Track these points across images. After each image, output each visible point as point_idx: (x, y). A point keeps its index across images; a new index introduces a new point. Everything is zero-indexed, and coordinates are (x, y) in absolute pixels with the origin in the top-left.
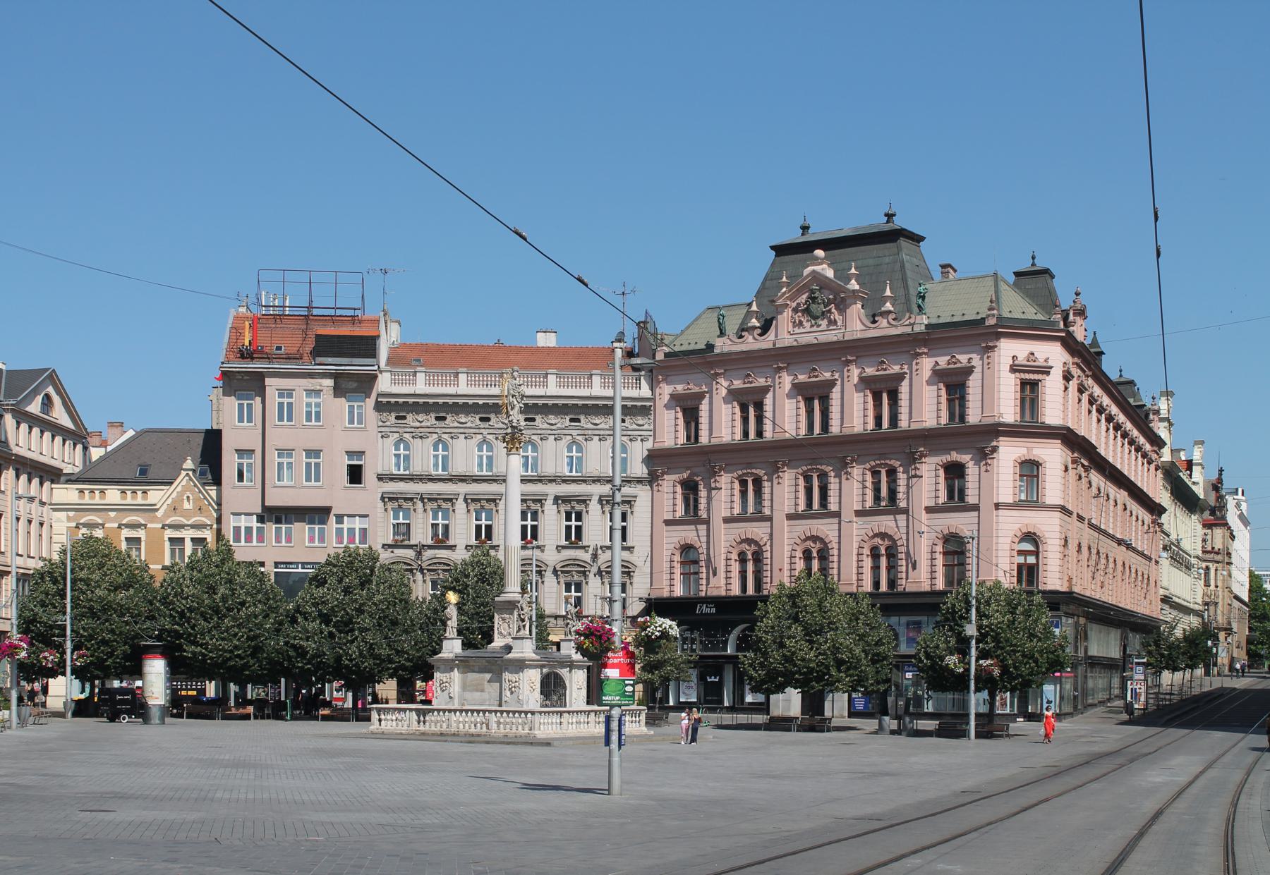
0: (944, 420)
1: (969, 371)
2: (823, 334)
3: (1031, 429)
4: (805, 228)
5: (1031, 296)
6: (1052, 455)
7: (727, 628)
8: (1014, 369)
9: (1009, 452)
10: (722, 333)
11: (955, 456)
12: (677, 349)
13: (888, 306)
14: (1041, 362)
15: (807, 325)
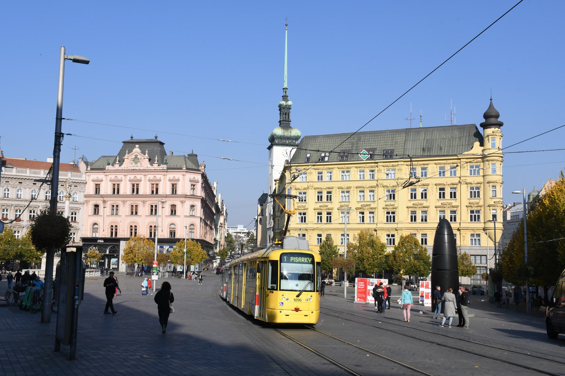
0: (171, 193)
1: (178, 180)
2: (138, 167)
3: (193, 196)
4: (132, 138)
5: (192, 161)
6: (198, 204)
7: (106, 246)
8: (190, 181)
9: (189, 202)
10: (109, 164)
11: (175, 203)
12: (93, 167)
13: (156, 162)
14: (196, 179)
15: (134, 164)
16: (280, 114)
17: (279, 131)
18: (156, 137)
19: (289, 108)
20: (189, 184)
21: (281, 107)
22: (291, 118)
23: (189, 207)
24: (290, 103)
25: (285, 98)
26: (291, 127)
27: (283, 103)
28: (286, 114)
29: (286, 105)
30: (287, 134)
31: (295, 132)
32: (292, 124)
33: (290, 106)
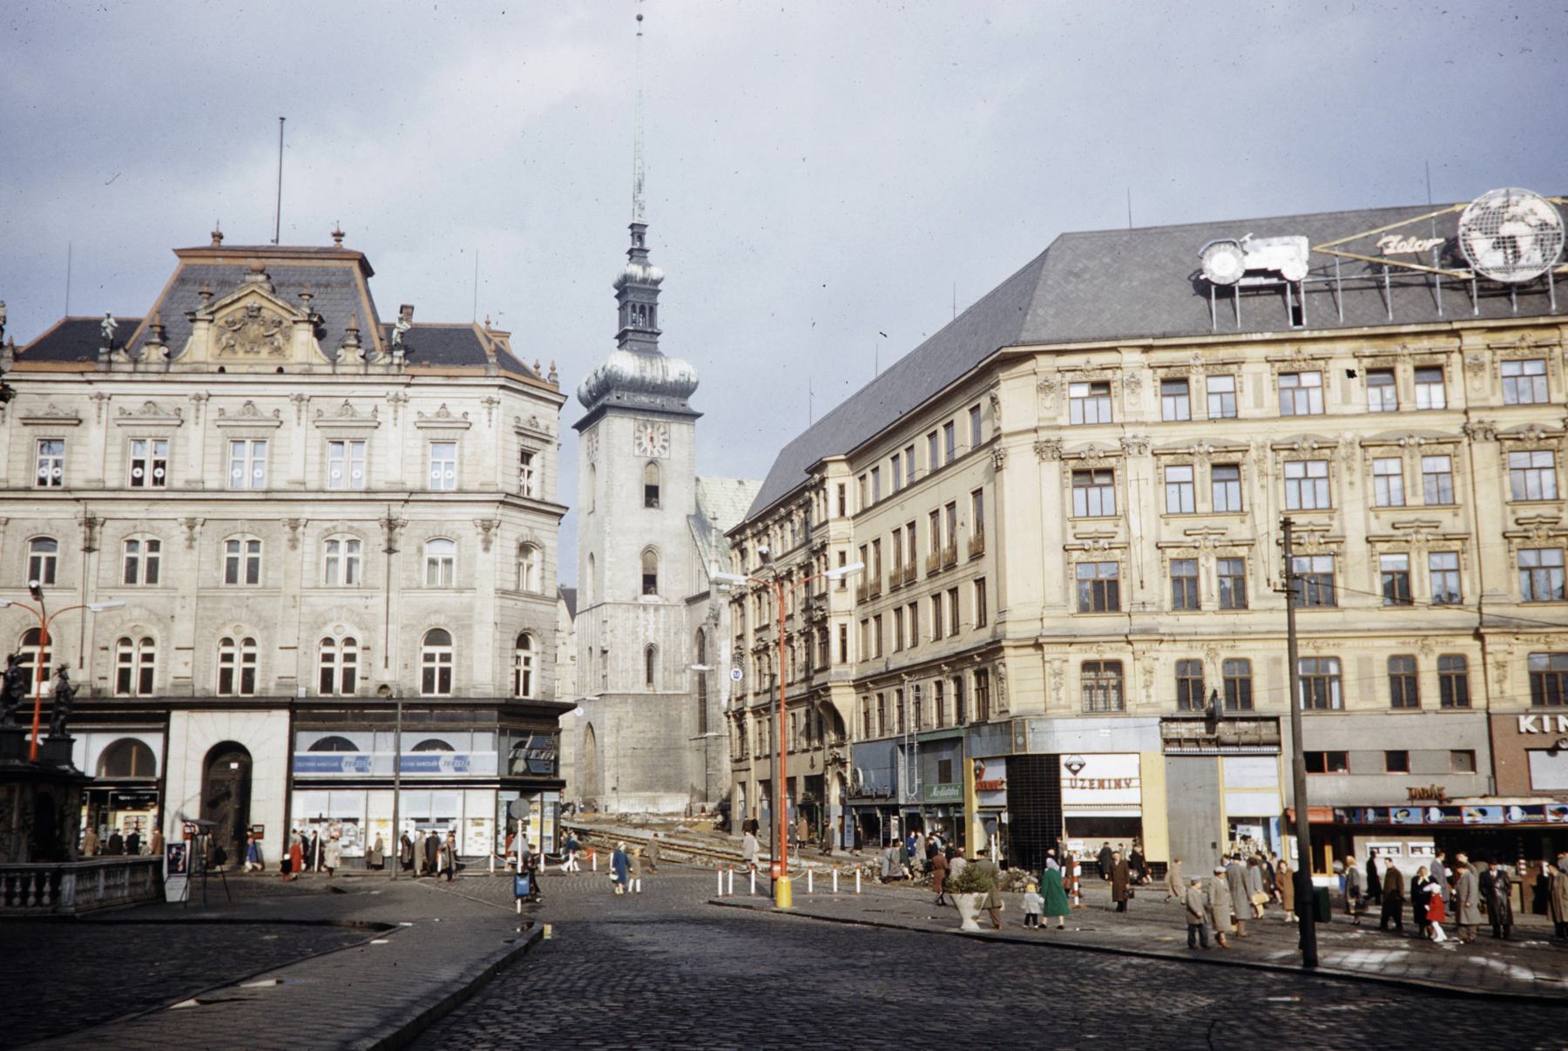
14: (542, 429)
16: (622, 308)
17: (627, 364)
18: (338, 236)
19: (652, 287)
20: (515, 445)
21: (624, 288)
22: (661, 324)
23: (513, 550)
24: (655, 272)
25: (638, 254)
26: (660, 354)
27: (636, 270)
28: (642, 308)
29: (644, 281)
30: (653, 371)
31: (674, 369)
32: (660, 347)
33: (657, 282)
